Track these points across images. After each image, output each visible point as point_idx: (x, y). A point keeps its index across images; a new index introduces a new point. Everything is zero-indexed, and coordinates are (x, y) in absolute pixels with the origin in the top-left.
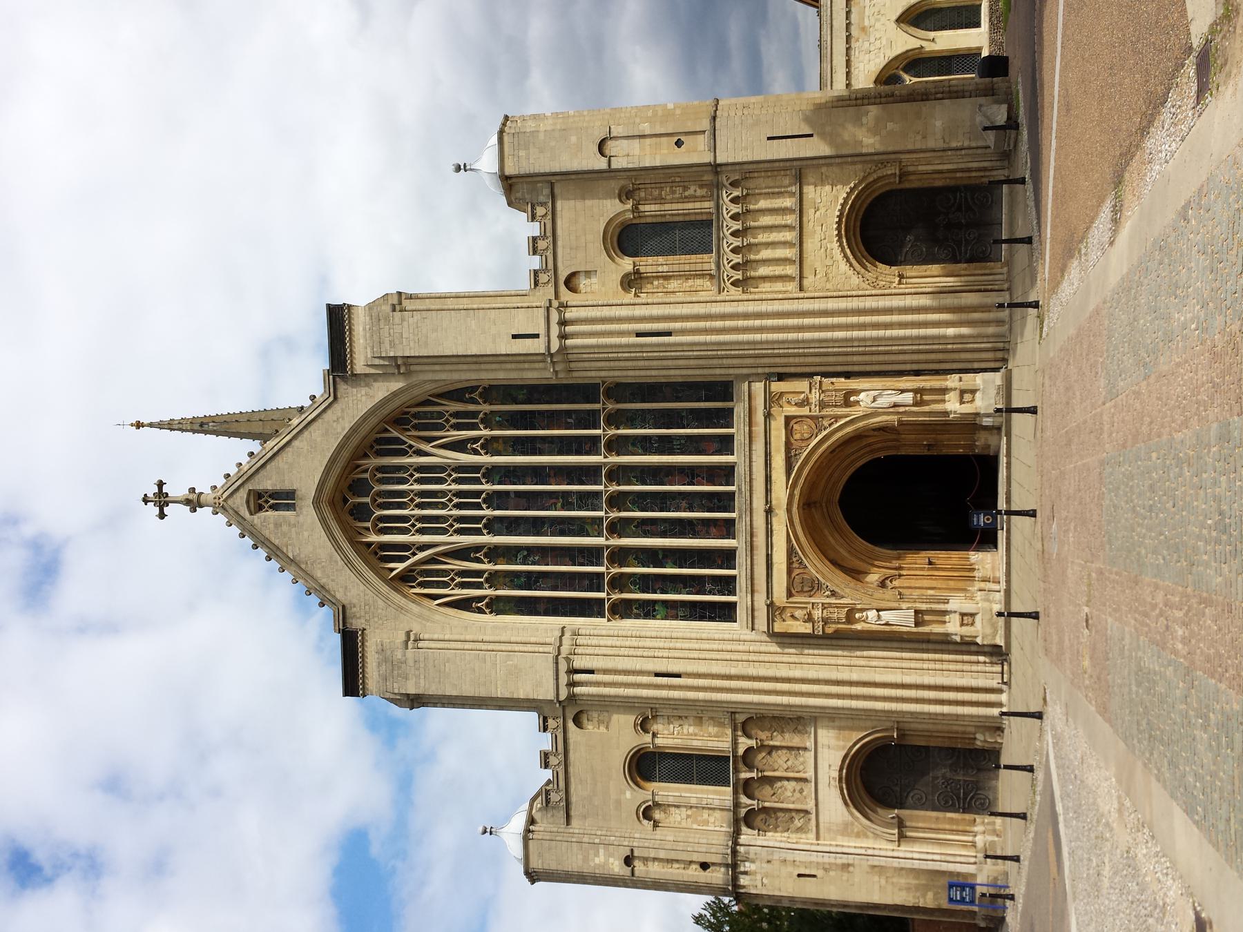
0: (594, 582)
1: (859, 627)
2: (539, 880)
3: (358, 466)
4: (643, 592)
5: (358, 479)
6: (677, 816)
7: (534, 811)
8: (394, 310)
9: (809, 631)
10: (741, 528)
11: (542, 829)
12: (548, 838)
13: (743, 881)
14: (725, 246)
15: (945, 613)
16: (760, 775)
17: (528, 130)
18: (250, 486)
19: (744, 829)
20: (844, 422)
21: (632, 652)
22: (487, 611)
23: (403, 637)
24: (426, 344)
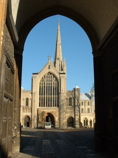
0: (42, 95)
10: (47, 108)
23: (38, 78)
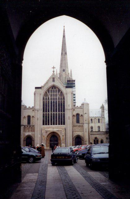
0: (46, 112)
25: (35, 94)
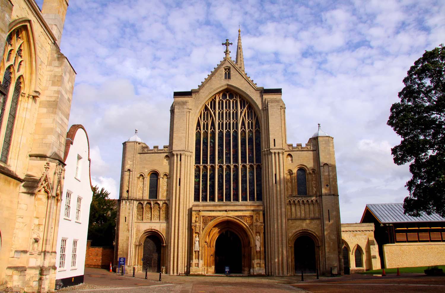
0: (205, 161)
1: (194, 235)
2: (124, 145)
3: (237, 96)
4: (202, 175)
5: (233, 96)
6: (141, 184)
7: (142, 144)
8: (281, 107)
9: (193, 222)
10: (221, 203)
11: (137, 146)
12: (135, 148)
13: (124, 202)
14: (300, 199)
15: (198, 259)
16: (152, 207)
17: (330, 144)
18: (231, 67)
19: (138, 202)
20: (251, 233)
21: (186, 172)
22: (197, 131)
23: (190, 108)
24: (272, 115)
25: (172, 111)
